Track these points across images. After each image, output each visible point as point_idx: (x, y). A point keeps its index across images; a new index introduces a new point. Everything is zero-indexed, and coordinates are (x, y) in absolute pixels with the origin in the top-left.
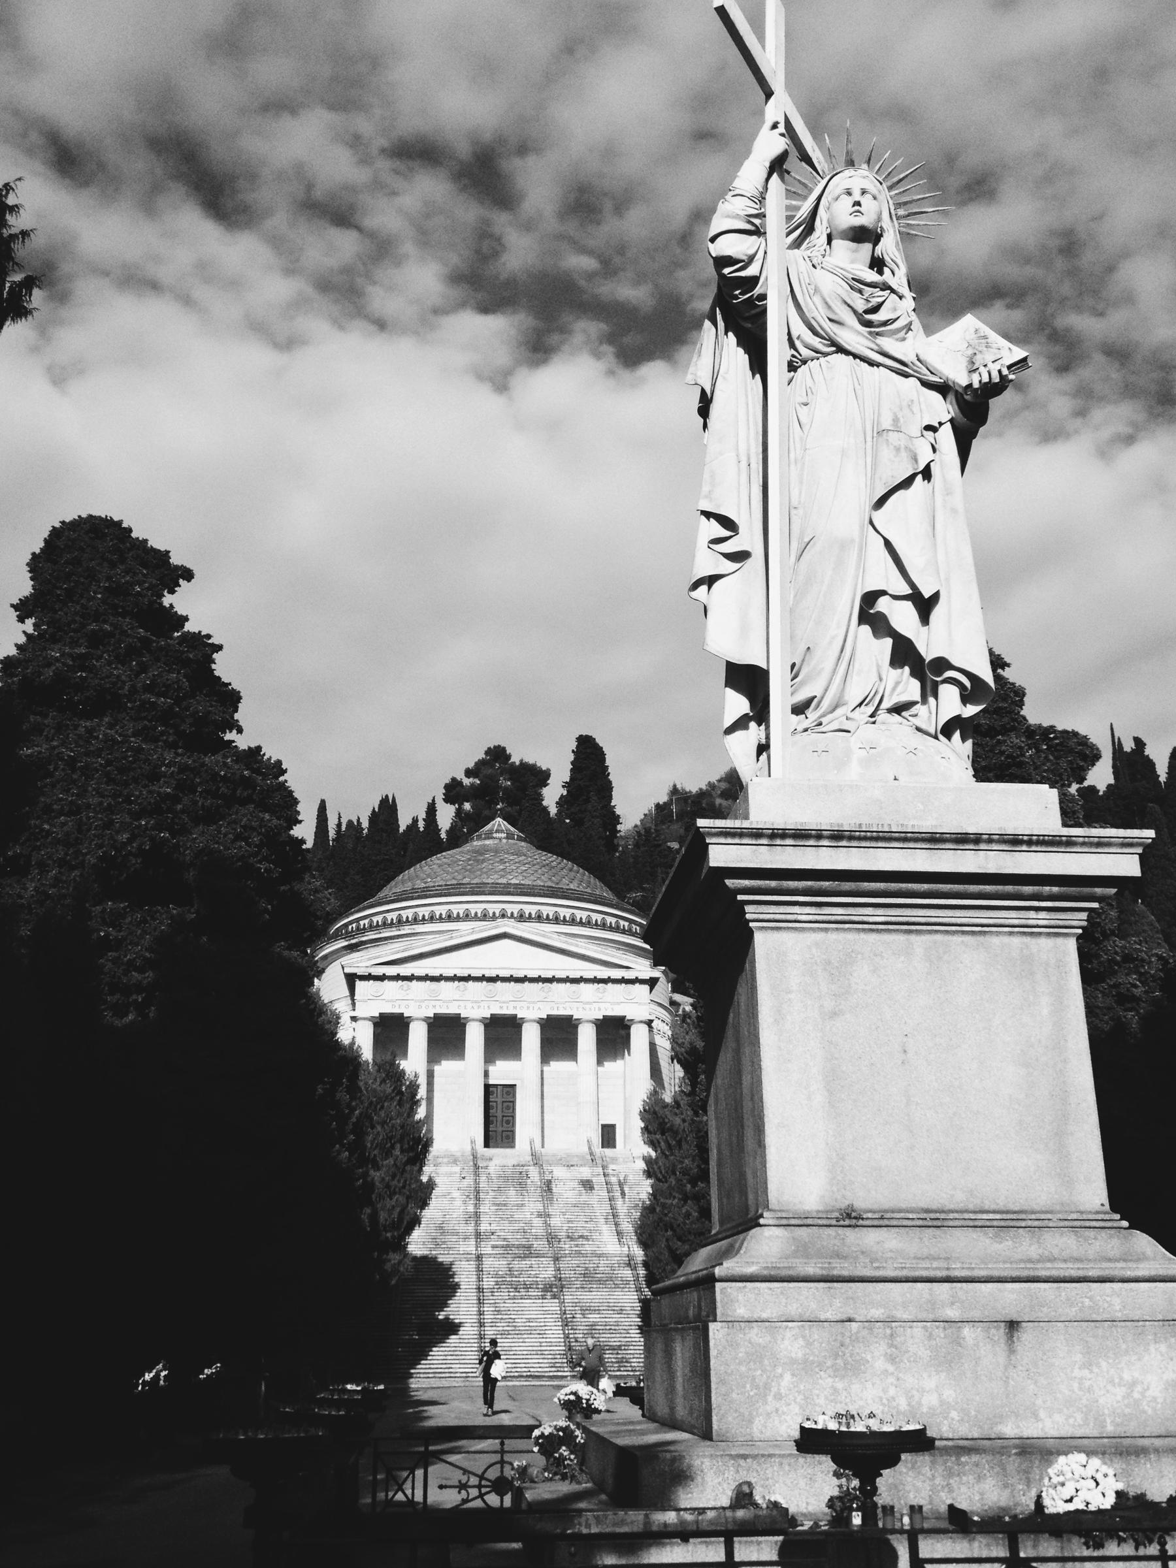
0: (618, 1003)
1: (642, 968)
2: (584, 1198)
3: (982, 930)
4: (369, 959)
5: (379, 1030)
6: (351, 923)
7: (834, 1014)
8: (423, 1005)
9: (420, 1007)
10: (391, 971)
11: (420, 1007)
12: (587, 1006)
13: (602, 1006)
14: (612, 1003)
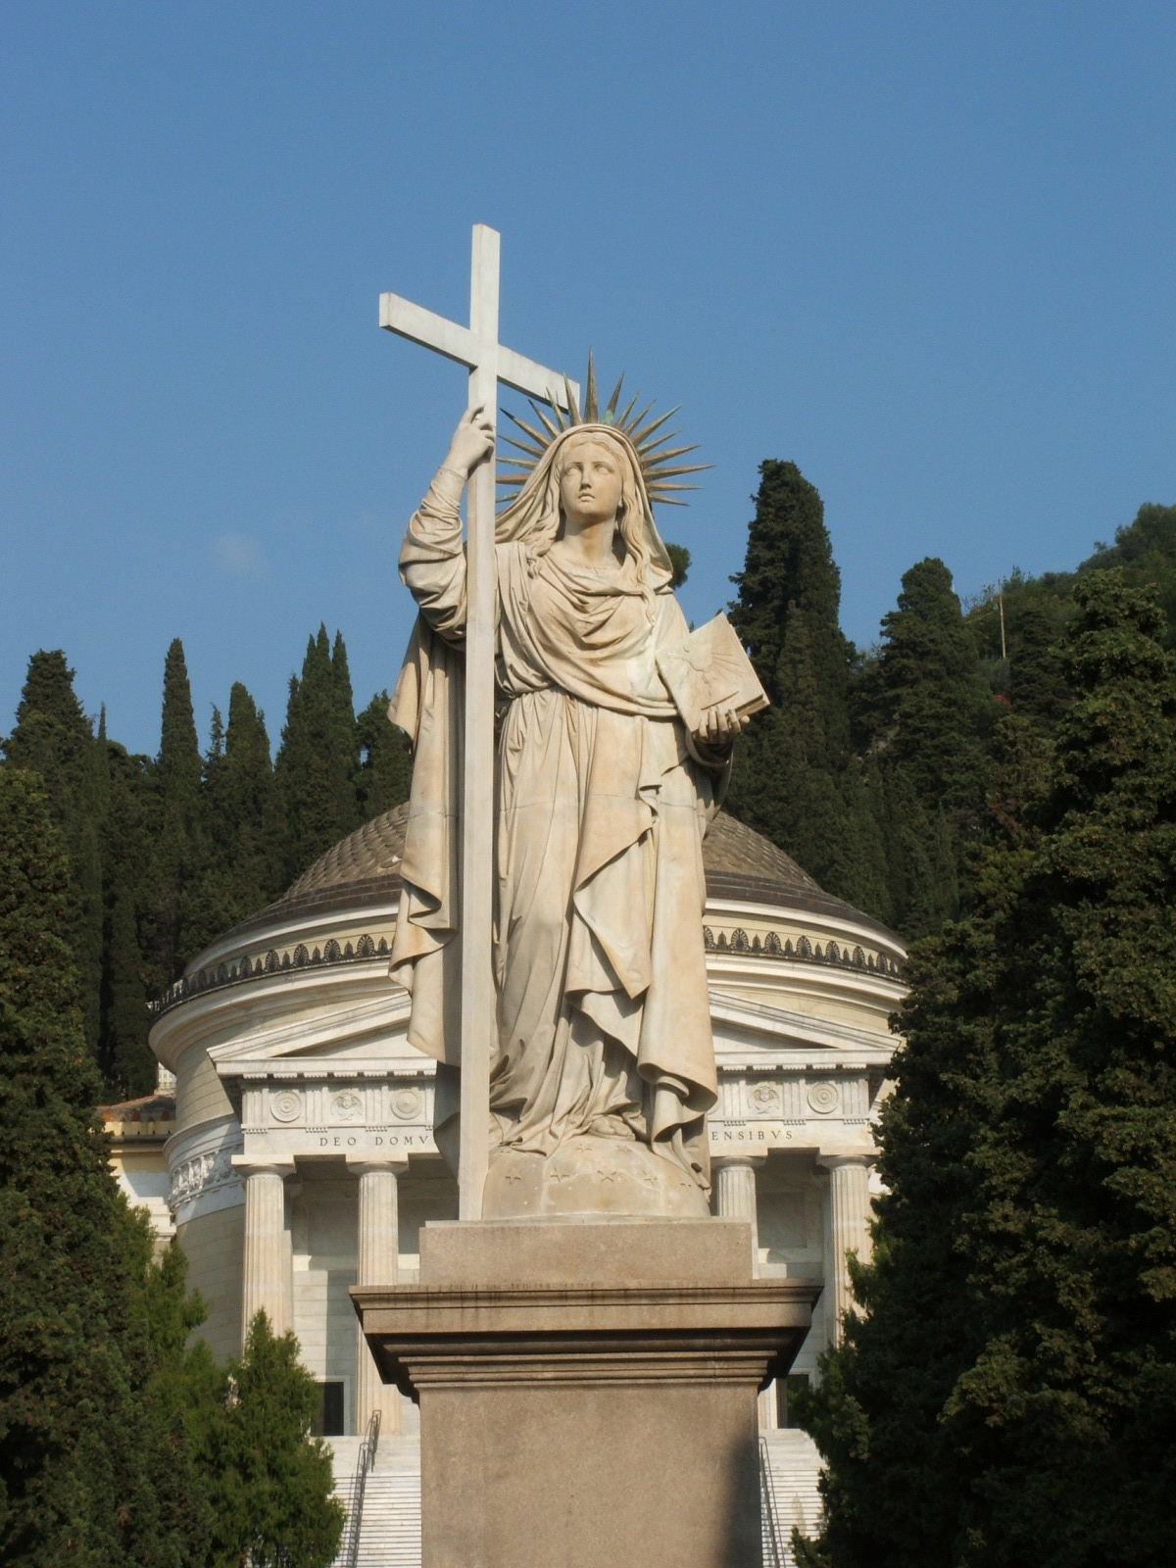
0: (801, 1122)
3: (658, 1383)
4: (269, 1044)
5: (298, 1189)
6: (232, 956)
7: (500, 1477)
8: (386, 1136)
9: (379, 1141)
12: (734, 1130)
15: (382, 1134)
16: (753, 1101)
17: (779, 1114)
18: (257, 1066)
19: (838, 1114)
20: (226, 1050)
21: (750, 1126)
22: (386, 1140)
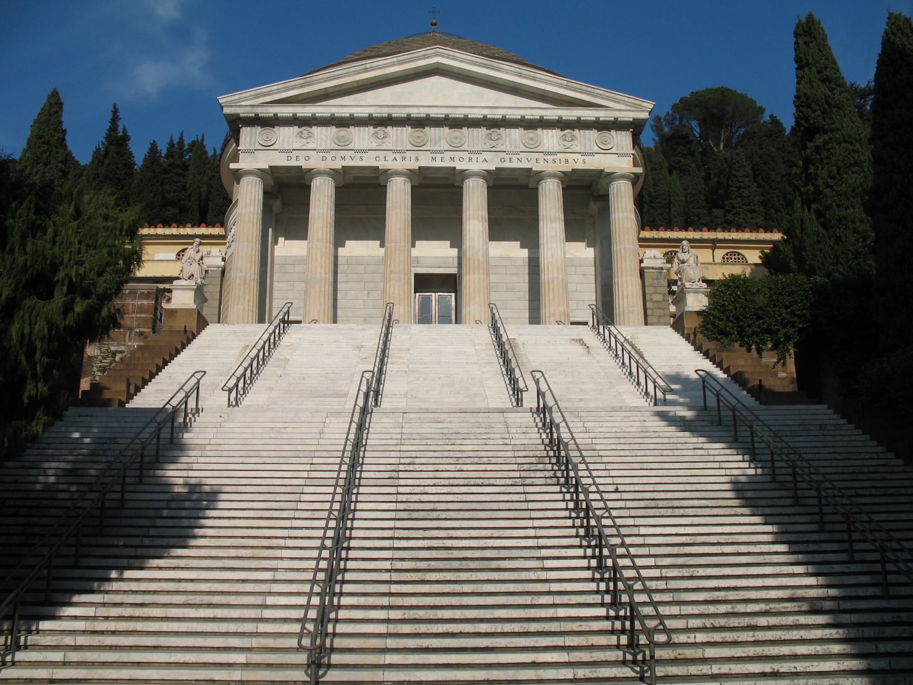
0: (592, 154)
1: (623, 107)
4: (257, 96)
8: (329, 156)
10: (285, 111)
11: (324, 159)
12: (550, 158)
13: (570, 157)
15: (326, 154)
16: (561, 142)
17: (578, 149)
18: (248, 109)
19: (613, 151)
20: (229, 99)
22: (329, 158)
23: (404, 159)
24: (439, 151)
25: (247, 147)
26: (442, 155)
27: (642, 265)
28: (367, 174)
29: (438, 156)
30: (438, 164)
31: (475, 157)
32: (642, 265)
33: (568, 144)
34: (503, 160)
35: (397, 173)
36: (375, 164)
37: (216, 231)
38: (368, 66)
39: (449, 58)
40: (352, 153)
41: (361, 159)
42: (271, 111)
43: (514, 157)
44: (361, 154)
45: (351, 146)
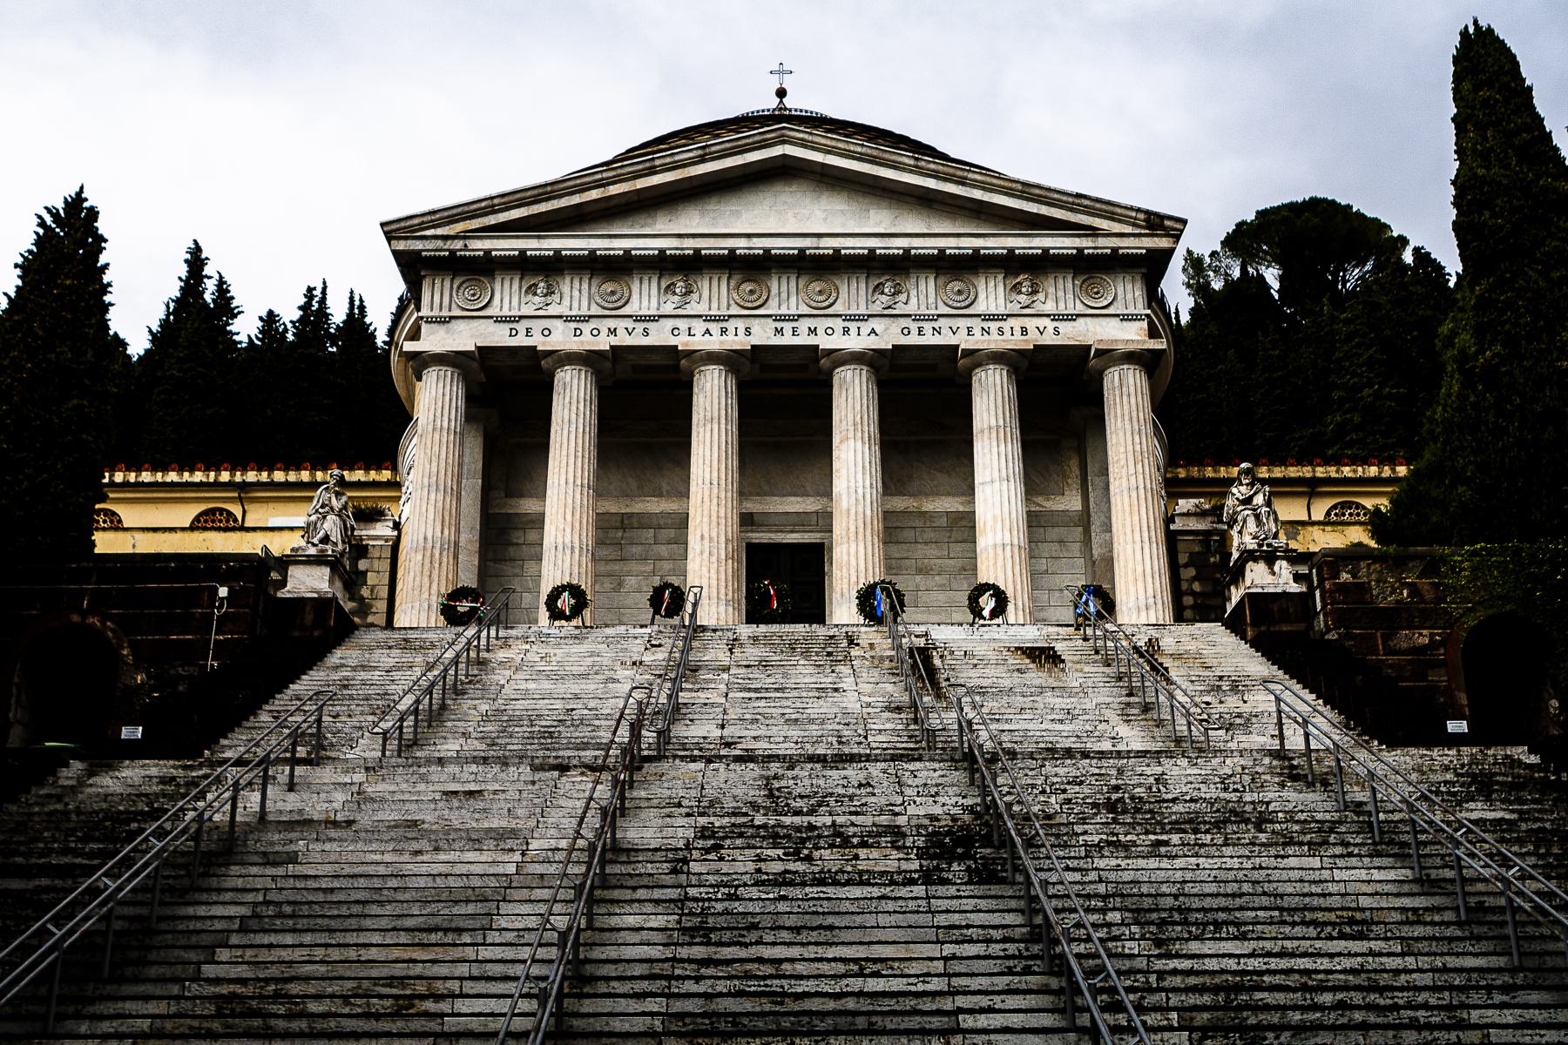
1: (1128, 229)
2: (1036, 676)
8: (586, 328)
11: (577, 333)
12: (994, 326)
13: (1031, 324)
14: (1056, 317)
15: (580, 325)
19: (1111, 311)
21: (1012, 322)
23: (724, 331)
24: (784, 319)
25: (436, 313)
26: (795, 324)
27: (1172, 527)
28: (656, 359)
29: (787, 326)
30: (787, 340)
31: (853, 325)
32: (1172, 527)
33: (1023, 298)
34: (906, 331)
35: (712, 358)
36: (672, 341)
37: (386, 475)
38: (657, 162)
39: (805, 147)
40: (629, 324)
41: (646, 332)
42: (479, 245)
43: (927, 326)
44: (646, 325)
45: (626, 311)
